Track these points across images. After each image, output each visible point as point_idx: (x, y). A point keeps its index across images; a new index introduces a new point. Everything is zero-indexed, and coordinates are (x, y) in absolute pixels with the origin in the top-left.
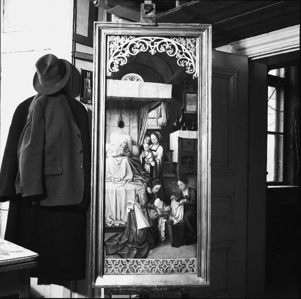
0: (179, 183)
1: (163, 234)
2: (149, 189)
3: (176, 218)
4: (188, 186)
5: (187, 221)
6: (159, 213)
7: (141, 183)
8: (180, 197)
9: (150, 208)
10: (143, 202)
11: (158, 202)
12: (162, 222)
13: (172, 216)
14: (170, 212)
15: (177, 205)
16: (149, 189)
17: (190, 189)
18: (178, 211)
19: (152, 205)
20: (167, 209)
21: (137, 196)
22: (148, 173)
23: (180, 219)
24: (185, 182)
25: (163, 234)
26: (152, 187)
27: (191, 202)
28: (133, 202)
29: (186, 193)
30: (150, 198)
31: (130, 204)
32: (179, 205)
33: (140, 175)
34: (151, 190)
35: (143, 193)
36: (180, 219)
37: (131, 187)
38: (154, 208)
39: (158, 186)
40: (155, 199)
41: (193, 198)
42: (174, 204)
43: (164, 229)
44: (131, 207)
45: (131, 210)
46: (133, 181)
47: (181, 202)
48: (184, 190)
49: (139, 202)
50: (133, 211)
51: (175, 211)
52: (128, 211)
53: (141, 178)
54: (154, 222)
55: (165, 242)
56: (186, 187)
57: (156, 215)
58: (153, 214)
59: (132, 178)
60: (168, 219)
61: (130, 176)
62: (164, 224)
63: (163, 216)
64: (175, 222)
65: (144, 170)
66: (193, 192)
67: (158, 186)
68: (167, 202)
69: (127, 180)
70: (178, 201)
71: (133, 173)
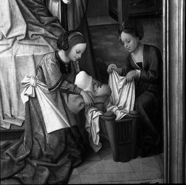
0: (124, 36)
1: (96, 140)
2: (61, 54)
3: (120, 109)
4: (143, 42)
5: (143, 112)
6: (86, 100)
7: (45, 43)
8: (127, 66)
9: (68, 92)
10: (53, 80)
11: (81, 79)
12: (94, 117)
13: (112, 104)
14: (108, 96)
15: (122, 83)
16: (61, 54)
17: (146, 48)
18: (123, 95)
19: (71, 86)
20: (101, 90)
21: (38, 69)
22: (56, 20)
23: (127, 108)
24: (137, 33)
25: (96, 140)
26: (67, 49)
27: (151, 75)
28: (32, 82)
29: (138, 58)
30: (66, 71)
31: (27, 85)
32: (126, 82)
33: (41, 24)
34: (67, 55)
35: (51, 62)
36: (127, 108)
37: (25, 51)
38: (76, 91)
39: (80, 47)
40: (76, 73)
41: (153, 66)
42: (116, 81)
43: (98, 130)
44: (30, 91)
45: (30, 97)
46: (27, 37)
47: (130, 75)
48: (135, 51)
49: (43, 80)
50: (33, 99)
51: (117, 96)
52: (25, 99)
53: (43, 31)
54: (78, 119)
55: (102, 153)
56: (139, 44)
57: (80, 105)
58: (73, 103)
59: (24, 32)
60: (104, 110)
61: (21, 29)
62: (97, 121)
63: (93, 105)
64: (120, 115)
65: (49, 14)
66: (153, 53)
67: (80, 47)
68: (101, 77)
69: (15, 38)
70: (123, 74)
71: (27, 23)
